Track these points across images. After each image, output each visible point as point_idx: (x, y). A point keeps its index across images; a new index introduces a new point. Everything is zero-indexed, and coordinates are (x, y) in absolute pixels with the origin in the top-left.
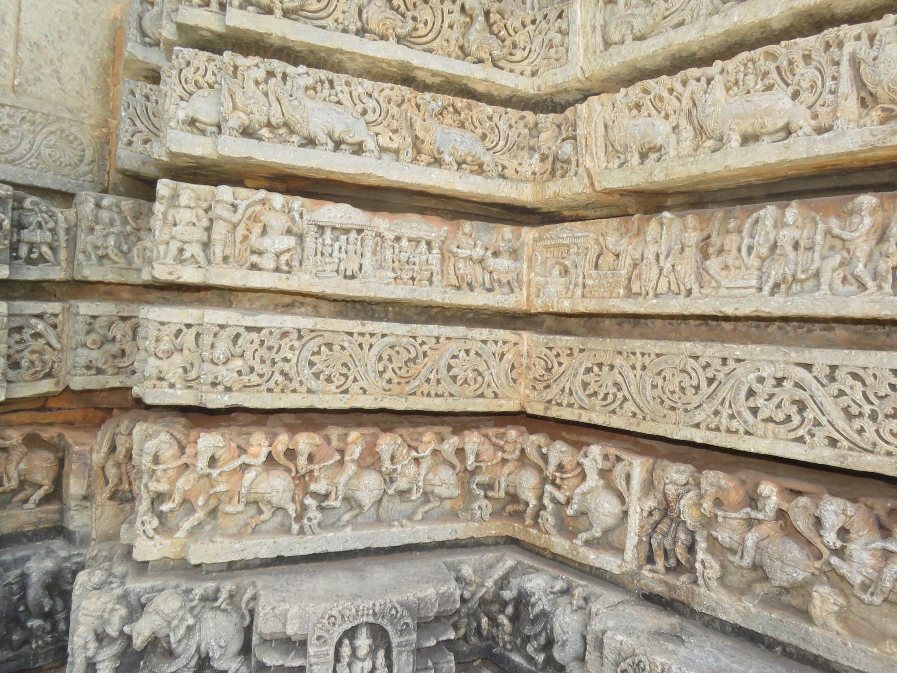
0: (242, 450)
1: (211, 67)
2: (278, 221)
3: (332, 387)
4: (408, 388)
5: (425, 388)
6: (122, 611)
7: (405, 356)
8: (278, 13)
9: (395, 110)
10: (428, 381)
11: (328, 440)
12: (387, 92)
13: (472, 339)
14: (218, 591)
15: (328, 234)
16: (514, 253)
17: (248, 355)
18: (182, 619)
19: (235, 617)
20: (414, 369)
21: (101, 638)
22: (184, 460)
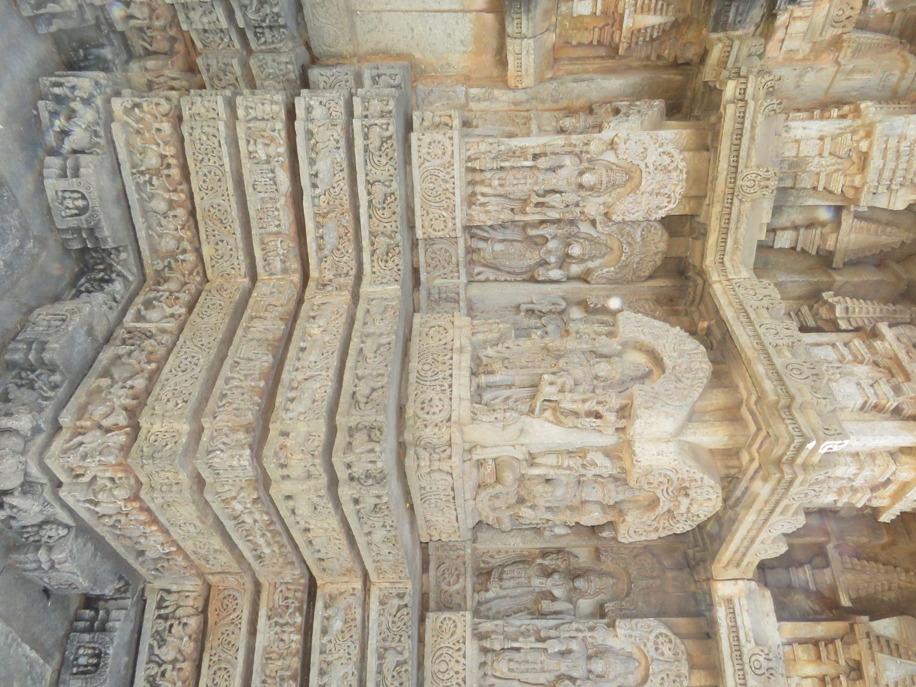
0: (166, 143)
1: (338, 114)
2: (272, 150)
3: (201, 183)
4: (207, 220)
5: (210, 230)
6: (85, 96)
7: (223, 218)
8: (365, 142)
9: (337, 202)
11: (181, 184)
12: (345, 198)
14: (100, 137)
15: (270, 175)
16: (285, 271)
17: (208, 142)
19: (88, 146)
21: (73, 88)
22: (159, 117)
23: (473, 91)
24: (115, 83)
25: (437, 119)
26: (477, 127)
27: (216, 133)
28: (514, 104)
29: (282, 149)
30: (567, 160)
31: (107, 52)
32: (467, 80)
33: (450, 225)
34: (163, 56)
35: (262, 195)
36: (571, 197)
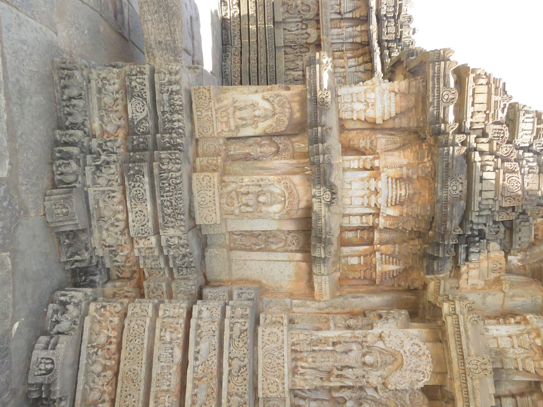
1: (217, 315)
2: (174, 336)
3: (127, 355)
5: (124, 386)
7: (134, 378)
8: (231, 333)
9: (209, 371)
10: (126, 387)
11: (114, 354)
12: (214, 368)
13: (139, 403)
14: (76, 325)
15: (170, 351)
17: (138, 330)
18: (70, 317)
20: (130, 382)
21: (72, 297)
22: (114, 313)
23: (295, 301)
24: (95, 293)
25: (274, 319)
26: (297, 323)
27: (144, 324)
28: (319, 309)
29: (180, 336)
30: (354, 347)
31: (97, 278)
32: (291, 295)
33: (281, 388)
34: (126, 280)
35: (163, 364)
36: (359, 372)
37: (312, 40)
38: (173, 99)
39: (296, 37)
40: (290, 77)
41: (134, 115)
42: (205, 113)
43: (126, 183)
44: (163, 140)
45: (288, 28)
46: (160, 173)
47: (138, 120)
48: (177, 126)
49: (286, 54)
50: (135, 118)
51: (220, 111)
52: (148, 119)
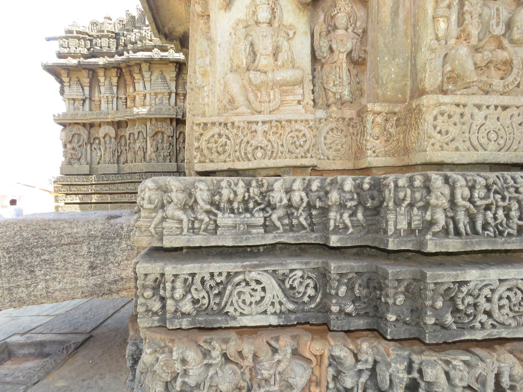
37: (112, 131)
38: (230, 202)
39: (108, 150)
40: (154, 155)
41: (271, 310)
42: (260, 139)
43: (479, 336)
44: (346, 228)
45: (98, 159)
46: (457, 233)
47: (284, 300)
48: (303, 194)
49: (126, 162)
50: (277, 306)
51: (256, 105)
52: (281, 270)
